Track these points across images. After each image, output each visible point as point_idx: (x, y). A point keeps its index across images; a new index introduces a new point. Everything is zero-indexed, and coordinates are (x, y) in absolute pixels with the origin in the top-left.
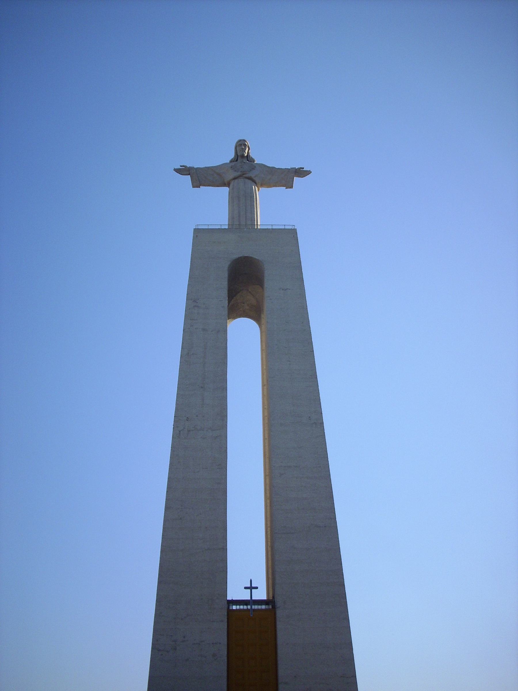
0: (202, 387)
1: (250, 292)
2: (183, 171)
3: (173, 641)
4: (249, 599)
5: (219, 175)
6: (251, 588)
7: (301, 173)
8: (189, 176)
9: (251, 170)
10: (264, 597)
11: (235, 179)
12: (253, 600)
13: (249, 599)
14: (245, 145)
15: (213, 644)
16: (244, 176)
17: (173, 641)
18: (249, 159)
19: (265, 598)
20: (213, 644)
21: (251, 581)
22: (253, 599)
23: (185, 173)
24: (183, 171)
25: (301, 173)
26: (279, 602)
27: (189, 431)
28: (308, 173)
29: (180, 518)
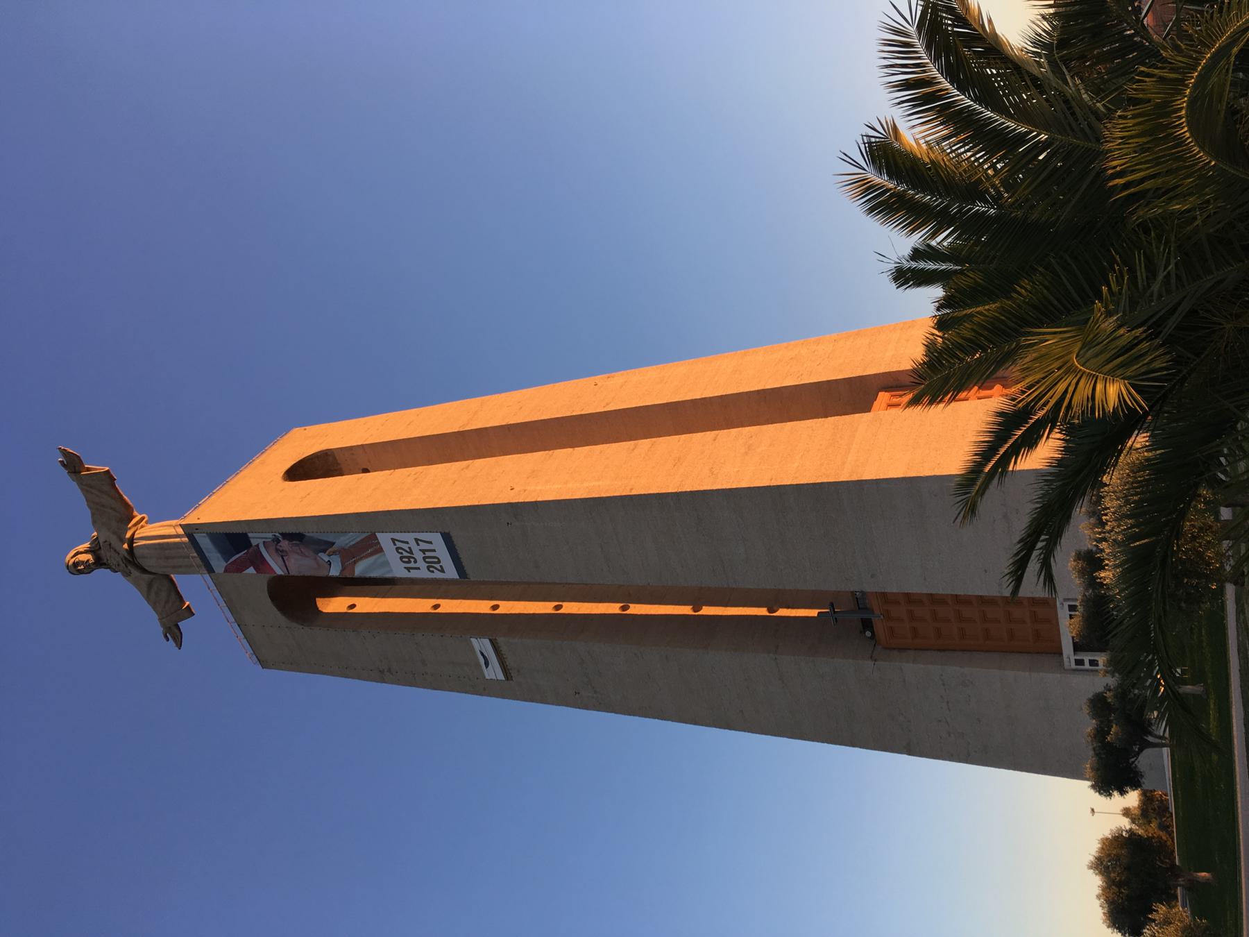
2: (174, 633)
3: (950, 735)
5: (150, 586)
7: (73, 465)
8: (179, 624)
9: (115, 551)
11: (144, 571)
14: (76, 564)
15: (944, 685)
16: (131, 560)
17: (950, 735)
18: (97, 548)
23: (176, 631)
24: (174, 633)
25: (73, 465)
27: (595, 692)
28: (65, 453)
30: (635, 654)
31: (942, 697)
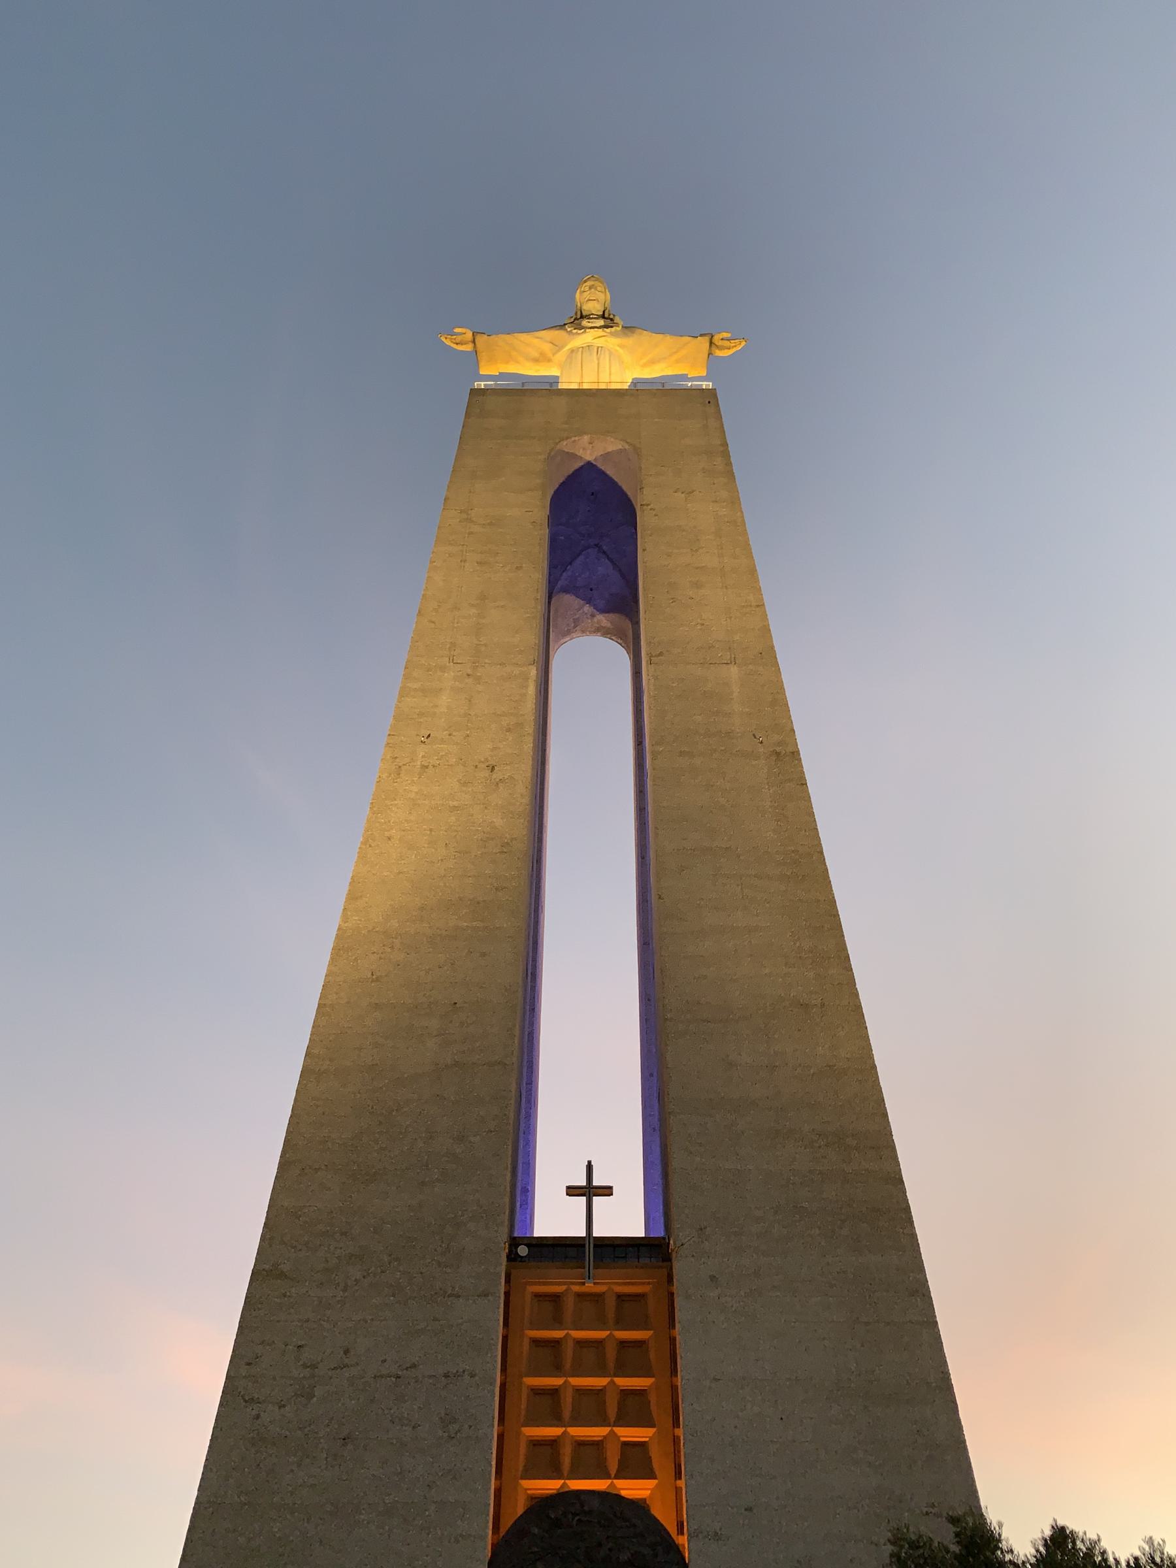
0: (468, 675)
1: (604, 552)
3: (305, 1366)
4: (583, 1234)
6: (589, 1191)
10: (634, 1227)
12: (596, 1238)
13: (583, 1234)
15: (446, 1376)
17: (305, 1366)
19: (640, 1232)
20: (446, 1376)
21: (589, 1167)
22: (595, 1234)
26: (682, 1238)
29: (374, 977)
30: (508, 843)
31: (414, 1366)
